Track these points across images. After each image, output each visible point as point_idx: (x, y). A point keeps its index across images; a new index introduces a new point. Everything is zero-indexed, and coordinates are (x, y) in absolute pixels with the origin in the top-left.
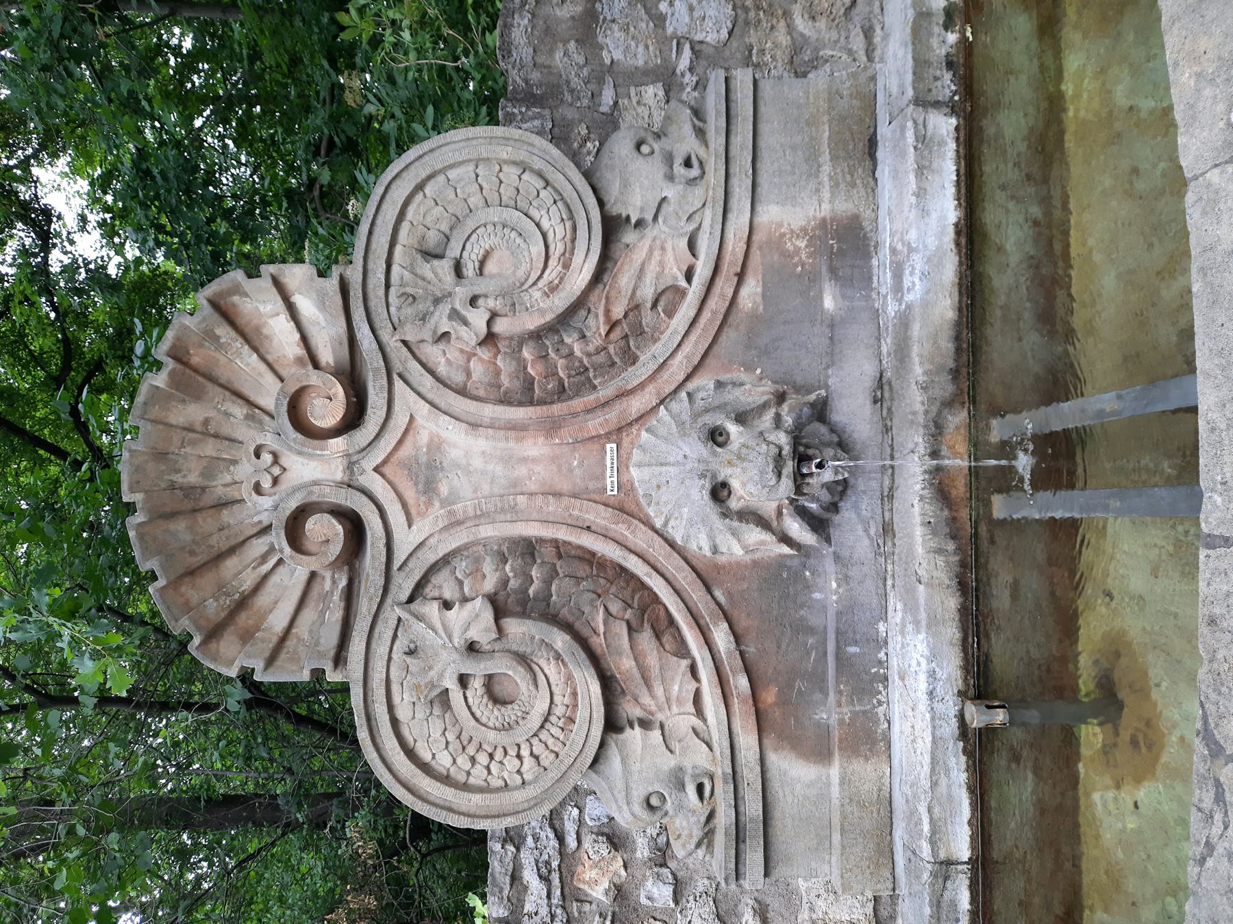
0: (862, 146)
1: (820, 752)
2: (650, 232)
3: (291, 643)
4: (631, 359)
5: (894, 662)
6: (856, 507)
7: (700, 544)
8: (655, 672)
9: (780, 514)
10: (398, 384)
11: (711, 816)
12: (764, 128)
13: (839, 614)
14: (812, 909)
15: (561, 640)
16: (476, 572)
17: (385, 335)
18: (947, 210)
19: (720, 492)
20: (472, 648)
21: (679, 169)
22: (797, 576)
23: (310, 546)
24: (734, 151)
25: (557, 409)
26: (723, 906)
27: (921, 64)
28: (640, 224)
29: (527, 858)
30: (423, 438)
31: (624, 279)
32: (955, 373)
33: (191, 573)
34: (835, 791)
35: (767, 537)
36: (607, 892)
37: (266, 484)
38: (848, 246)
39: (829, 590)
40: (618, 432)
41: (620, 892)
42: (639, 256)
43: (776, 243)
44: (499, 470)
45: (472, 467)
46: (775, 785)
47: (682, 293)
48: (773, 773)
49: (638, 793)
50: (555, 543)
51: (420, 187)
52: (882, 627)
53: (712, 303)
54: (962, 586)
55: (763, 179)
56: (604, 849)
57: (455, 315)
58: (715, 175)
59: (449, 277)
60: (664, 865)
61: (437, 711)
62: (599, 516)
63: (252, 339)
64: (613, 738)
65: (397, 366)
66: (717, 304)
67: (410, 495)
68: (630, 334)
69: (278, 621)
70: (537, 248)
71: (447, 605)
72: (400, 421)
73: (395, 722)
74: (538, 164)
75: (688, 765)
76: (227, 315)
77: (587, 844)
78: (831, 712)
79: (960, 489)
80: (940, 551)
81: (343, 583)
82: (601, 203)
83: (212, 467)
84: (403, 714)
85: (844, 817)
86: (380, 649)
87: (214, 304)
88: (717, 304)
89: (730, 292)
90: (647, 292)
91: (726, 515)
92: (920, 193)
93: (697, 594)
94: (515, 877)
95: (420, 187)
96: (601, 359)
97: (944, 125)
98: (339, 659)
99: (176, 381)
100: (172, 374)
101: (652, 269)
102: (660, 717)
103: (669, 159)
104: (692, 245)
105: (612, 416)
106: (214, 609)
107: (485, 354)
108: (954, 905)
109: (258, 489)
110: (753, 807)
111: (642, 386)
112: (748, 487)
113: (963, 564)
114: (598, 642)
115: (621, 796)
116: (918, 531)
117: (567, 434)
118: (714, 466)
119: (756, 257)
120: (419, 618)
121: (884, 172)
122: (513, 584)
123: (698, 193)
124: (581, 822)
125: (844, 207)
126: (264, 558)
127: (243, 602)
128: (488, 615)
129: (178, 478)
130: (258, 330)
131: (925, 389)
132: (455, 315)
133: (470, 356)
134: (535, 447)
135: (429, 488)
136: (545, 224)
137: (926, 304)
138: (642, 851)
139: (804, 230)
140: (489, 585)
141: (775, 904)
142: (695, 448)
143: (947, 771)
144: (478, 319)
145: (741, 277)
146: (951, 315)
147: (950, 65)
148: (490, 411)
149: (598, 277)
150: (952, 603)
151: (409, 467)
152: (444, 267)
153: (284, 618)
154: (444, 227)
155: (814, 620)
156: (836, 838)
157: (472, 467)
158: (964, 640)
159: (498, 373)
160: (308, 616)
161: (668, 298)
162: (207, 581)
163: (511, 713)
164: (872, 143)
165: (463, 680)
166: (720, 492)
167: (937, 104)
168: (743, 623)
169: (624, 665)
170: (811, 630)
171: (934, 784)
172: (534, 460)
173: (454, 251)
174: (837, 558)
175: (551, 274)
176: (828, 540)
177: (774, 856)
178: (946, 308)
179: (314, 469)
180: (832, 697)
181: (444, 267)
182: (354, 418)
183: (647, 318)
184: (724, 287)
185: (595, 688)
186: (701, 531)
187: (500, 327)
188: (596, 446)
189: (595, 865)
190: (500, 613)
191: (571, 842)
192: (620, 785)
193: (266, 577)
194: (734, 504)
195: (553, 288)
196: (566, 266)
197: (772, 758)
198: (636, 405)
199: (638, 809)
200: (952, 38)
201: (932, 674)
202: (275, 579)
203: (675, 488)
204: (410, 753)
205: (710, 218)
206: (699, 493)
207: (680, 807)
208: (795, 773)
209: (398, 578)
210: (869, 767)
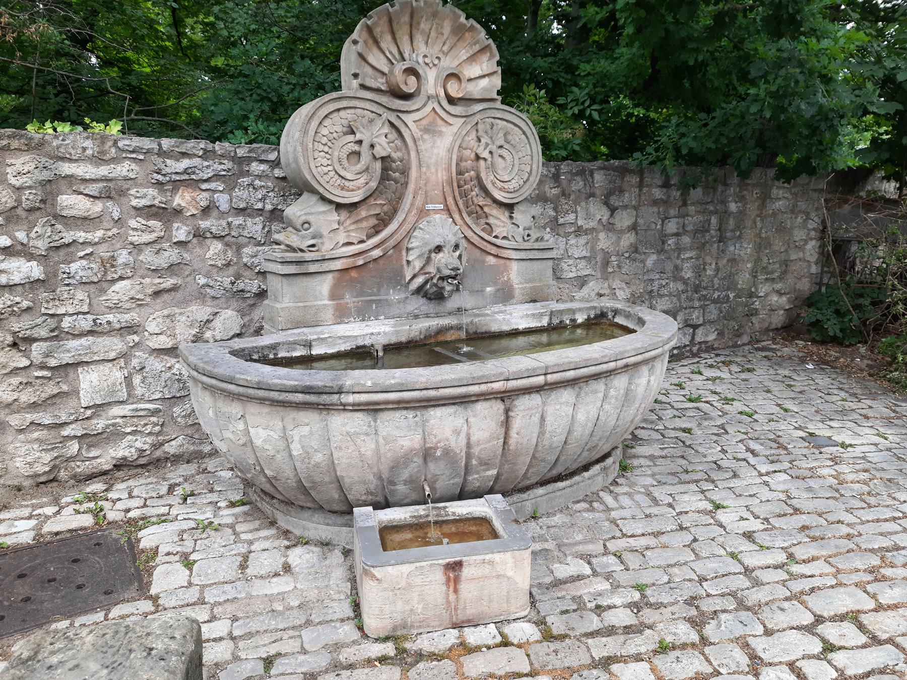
0: (534, 297)
1: (333, 296)
2: (508, 221)
3: (363, 63)
4: (470, 214)
5: (369, 323)
6: (424, 304)
7: (414, 243)
8: (360, 225)
9: (426, 273)
10: (463, 120)
11: (302, 251)
12: (539, 262)
13: (387, 300)
14: (181, 314)
15: (373, 184)
16: (397, 149)
18: (522, 325)
19: (439, 249)
20: (372, 146)
21: (527, 232)
22: (398, 283)
24: (533, 252)
25: (455, 185)
26: (176, 268)
27: (561, 312)
28: (511, 218)
29: (196, 161)
30: (444, 129)
32: (476, 333)
33: (390, 21)
34: (319, 303)
35: (417, 269)
36: (179, 205)
37: (427, 60)
38: (505, 295)
39: (395, 296)
40: (448, 210)
41: (178, 212)
43: (506, 269)
44: (433, 160)
45: (437, 149)
46: (319, 278)
47: (490, 234)
48: (324, 277)
49: (311, 218)
50: (407, 183)
52: (382, 317)
53: (489, 245)
54: (409, 342)
55: (525, 263)
56: (204, 204)
57: (487, 145)
58: (527, 245)
59: (499, 143)
60: (194, 236)
61: (345, 129)
62: (419, 202)
63: (472, 58)
64: (334, 207)
66: (489, 248)
67: (424, 122)
68: (479, 214)
69: (371, 59)
70: (506, 178)
72: (451, 120)
73: (338, 110)
75: (325, 240)
76: (483, 50)
77: (205, 194)
78: (349, 299)
79: (441, 338)
80: (421, 333)
81: (383, 88)
84: (342, 113)
85: (311, 307)
86: (368, 105)
87: (488, 46)
88: (489, 248)
89: (492, 252)
90: (491, 221)
91: (430, 251)
92: (527, 315)
93: (392, 243)
94: (184, 155)
95: (524, 133)
96: (471, 203)
97: (545, 322)
99: (462, 26)
100: (465, 25)
101: (498, 223)
102: (341, 228)
103: (529, 229)
104: (504, 238)
105: (453, 207)
106: (377, 31)
107: (473, 156)
108: (294, 350)
109: (425, 56)
110: (313, 268)
111: (463, 218)
112: (441, 259)
113: (416, 341)
114: (372, 201)
115: (308, 210)
116: (427, 324)
117: (447, 189)
118: (448, 246)
119: (502, 261)
120: (383, 124)
121: (527, 306)
122: (394, 165)
123: (520, 239)
124: (215, 191)
125: (517, 293)
126: (391, 53)
127: (376, 42)
128: (384, 154)
129: (424, 19)
130: (475, 60)
131: (471, 322)
132: (487, 145)
133: (471, 150)
134: (442, 176)
135: (426, 130)
136: (513, 181)
137: (496, 320)
138: (204, 224)
139: (509, 279)
141: (179, 295)
142: (453, 240)
143: (345, 343)
144: (485, 154)
145: (497, 256)
146: (493, 330)
147: (561, 322)
148: (455, 157)
149: (495, 201)
150: (403, 339)
151: (433, 123)
152: (501, 142)
154: (513, 142)
155: (383, 291)
156: (301, 304)
157: (437, 149)
158: (391, 345)
159: (466, 161)
161: (489, 228)
162: (386, 28)
163: (345, 162)
164: (534, 301)
165: (360, 142)
166: (439, 249)
167: (551, 319)
168: (381, 262)
169: (363, 212)
170: (379, 290)
171: (340, 338)
172: (437, 175)
174: (407, 298)
176: (413, 294)
177: (291, 278)
178: (495, 328)
180: (356, 299)
182: (451, 101)
183: (483, 221)
184: (494, 250)
185: (356, 200)
186: (419, 241)
187: (482, 162)
188: (442, 200)
189: (194, 199)
190: (383, 158)
192: (313, 210)
194: (433, 255)
196: (500, 189)
197: (330, 276)
198: (456, 216)
199: (303, 218)
200: (568, 322)
201: (379, 334)
202: (382, 56)
203: (434, 231)
205: (513, 244)
206: (438, 241)
207: (303, 237)
208: (324, 285)
210: (331, 316)
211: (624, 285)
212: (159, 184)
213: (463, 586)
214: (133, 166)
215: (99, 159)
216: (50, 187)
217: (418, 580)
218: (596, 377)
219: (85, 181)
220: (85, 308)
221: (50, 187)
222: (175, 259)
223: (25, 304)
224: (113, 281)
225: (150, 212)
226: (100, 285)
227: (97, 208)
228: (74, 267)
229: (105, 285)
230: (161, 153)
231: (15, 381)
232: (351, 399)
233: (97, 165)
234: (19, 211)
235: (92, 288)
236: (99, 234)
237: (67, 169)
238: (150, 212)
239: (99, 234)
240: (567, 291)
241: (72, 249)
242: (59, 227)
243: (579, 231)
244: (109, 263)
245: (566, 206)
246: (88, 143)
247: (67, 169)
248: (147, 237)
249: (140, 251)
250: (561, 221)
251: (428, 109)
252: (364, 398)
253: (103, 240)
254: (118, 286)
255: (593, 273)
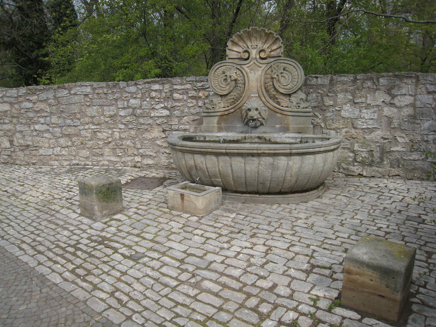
1: (218, 123)
2: (288, 101)
4: (271, 98)
15: (231, 89)
17: (273, 63)
20: (230, 77)
23: (244, 54)
28: (290, 100)
31: (281, 97)
37: (253, 47)
38: (286, 130)
41: (200, 97)
42: (285, 99)
46: (214, 117)
47: (280, 105)
51: (294, 67)
58: (296, 110)
65: (269, 65)
66: (277, 110)
67: (251, 67)
68: (274, 98)
70: (285, 84)
71: (236, 73)
72: (261, 65)
74: (298, 84)
78: (223, 125)
82: (293, 93)
83: (256, 38)
86: (230, 64)
88: (277, 110)
90: (279, 100)
93: (238, 107)
95: (294, 67)
98: (229, 59)
101: (283, 101)
105: (261, 95)
109: (252, 46)
110: (211, 114)
119: (284, 116)
122: (239, 82)
124: (209, 91)
125: (291, 129)
140: (239, 79)
144: (275, 76)
145: (281, 114)
150: (236, 139)
152: (282, 71)
153: (234, 51)
157: (255, 76)
160: (235, 53)
161: (279, 103)
163: (223, 82)
164: (300, 133)
169: (228, 97)
173: (285, 72)
175: (282, 86)
179: (254, 53)
181: (282, 71)
182: (261, 58)
183: (276, 100)
184: (280, 111)
185: (225, 93)
188: (257, 93)
191: (207, 90)
193: (241, 46)
195: (280, 87)
197: (217, 117)
198: (263, 99)
204: (217, 69)
208: (216, 120)
209: (240, 66)
211: (404, 135)
212: (195, 90)
213: (185, 201)
214: (190, 85)
215: (182, 84)
216: (172, 91)
217: (175, 196)
218: (253, 155)
219: (179, 90)
220: (177, 124)
221: (172, 91)
222: (198, 111)
223: (165, 121)
224: (184, 117)
225: (193, 98)
226: (180, 118)
227: (181, 97)
228: (175, 112)
229: (182, 118)
230: (197, 81)
231: (162, 140)
232: (177, 147)
233: (181, 86)
234: (166, 98)
235: (179, 118)
236: (181, 104)
237: (175, 87)
238: (193, 98)
239: (181, 104)
240: (361, 134)
241: (175, 108)
242: (173, 102)
243: (368, 106)
244: (182, 112)
245: (359, 95)
246: (179, 80)
247: (175, 87)
248: (191, 105)
249: (190, 108)
250: (356, 101)
251: (252, 63)
252: (179, 148)
253: (182, 105)
254: (185, 118)
255: (378, 127)
